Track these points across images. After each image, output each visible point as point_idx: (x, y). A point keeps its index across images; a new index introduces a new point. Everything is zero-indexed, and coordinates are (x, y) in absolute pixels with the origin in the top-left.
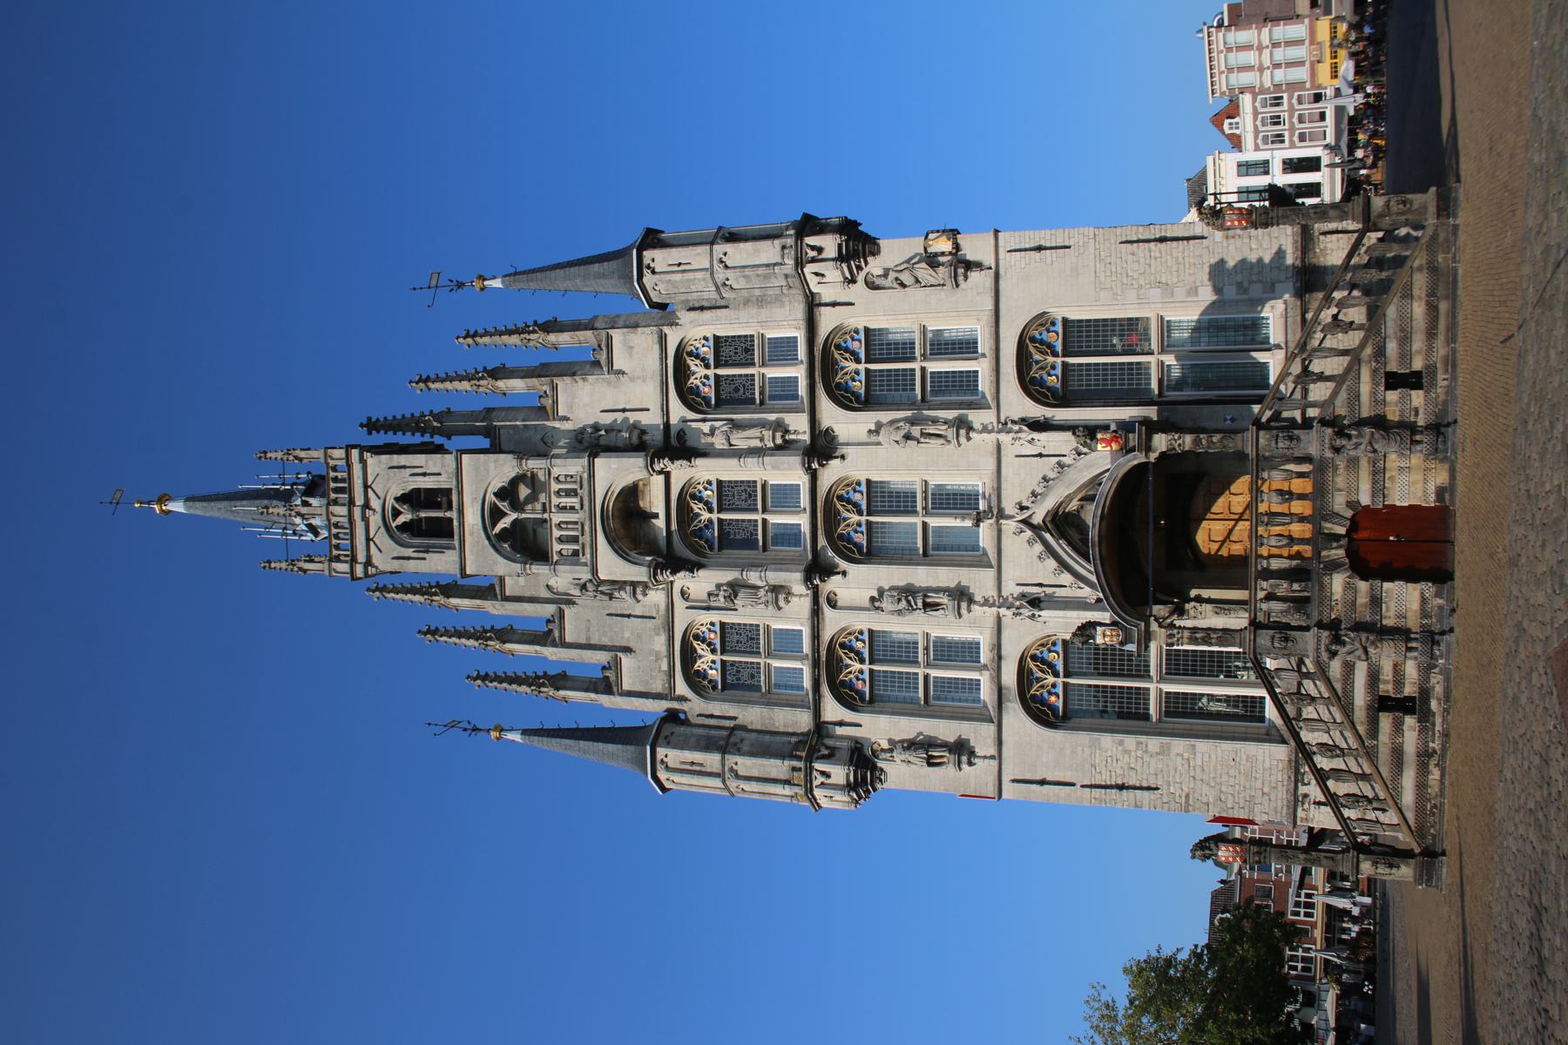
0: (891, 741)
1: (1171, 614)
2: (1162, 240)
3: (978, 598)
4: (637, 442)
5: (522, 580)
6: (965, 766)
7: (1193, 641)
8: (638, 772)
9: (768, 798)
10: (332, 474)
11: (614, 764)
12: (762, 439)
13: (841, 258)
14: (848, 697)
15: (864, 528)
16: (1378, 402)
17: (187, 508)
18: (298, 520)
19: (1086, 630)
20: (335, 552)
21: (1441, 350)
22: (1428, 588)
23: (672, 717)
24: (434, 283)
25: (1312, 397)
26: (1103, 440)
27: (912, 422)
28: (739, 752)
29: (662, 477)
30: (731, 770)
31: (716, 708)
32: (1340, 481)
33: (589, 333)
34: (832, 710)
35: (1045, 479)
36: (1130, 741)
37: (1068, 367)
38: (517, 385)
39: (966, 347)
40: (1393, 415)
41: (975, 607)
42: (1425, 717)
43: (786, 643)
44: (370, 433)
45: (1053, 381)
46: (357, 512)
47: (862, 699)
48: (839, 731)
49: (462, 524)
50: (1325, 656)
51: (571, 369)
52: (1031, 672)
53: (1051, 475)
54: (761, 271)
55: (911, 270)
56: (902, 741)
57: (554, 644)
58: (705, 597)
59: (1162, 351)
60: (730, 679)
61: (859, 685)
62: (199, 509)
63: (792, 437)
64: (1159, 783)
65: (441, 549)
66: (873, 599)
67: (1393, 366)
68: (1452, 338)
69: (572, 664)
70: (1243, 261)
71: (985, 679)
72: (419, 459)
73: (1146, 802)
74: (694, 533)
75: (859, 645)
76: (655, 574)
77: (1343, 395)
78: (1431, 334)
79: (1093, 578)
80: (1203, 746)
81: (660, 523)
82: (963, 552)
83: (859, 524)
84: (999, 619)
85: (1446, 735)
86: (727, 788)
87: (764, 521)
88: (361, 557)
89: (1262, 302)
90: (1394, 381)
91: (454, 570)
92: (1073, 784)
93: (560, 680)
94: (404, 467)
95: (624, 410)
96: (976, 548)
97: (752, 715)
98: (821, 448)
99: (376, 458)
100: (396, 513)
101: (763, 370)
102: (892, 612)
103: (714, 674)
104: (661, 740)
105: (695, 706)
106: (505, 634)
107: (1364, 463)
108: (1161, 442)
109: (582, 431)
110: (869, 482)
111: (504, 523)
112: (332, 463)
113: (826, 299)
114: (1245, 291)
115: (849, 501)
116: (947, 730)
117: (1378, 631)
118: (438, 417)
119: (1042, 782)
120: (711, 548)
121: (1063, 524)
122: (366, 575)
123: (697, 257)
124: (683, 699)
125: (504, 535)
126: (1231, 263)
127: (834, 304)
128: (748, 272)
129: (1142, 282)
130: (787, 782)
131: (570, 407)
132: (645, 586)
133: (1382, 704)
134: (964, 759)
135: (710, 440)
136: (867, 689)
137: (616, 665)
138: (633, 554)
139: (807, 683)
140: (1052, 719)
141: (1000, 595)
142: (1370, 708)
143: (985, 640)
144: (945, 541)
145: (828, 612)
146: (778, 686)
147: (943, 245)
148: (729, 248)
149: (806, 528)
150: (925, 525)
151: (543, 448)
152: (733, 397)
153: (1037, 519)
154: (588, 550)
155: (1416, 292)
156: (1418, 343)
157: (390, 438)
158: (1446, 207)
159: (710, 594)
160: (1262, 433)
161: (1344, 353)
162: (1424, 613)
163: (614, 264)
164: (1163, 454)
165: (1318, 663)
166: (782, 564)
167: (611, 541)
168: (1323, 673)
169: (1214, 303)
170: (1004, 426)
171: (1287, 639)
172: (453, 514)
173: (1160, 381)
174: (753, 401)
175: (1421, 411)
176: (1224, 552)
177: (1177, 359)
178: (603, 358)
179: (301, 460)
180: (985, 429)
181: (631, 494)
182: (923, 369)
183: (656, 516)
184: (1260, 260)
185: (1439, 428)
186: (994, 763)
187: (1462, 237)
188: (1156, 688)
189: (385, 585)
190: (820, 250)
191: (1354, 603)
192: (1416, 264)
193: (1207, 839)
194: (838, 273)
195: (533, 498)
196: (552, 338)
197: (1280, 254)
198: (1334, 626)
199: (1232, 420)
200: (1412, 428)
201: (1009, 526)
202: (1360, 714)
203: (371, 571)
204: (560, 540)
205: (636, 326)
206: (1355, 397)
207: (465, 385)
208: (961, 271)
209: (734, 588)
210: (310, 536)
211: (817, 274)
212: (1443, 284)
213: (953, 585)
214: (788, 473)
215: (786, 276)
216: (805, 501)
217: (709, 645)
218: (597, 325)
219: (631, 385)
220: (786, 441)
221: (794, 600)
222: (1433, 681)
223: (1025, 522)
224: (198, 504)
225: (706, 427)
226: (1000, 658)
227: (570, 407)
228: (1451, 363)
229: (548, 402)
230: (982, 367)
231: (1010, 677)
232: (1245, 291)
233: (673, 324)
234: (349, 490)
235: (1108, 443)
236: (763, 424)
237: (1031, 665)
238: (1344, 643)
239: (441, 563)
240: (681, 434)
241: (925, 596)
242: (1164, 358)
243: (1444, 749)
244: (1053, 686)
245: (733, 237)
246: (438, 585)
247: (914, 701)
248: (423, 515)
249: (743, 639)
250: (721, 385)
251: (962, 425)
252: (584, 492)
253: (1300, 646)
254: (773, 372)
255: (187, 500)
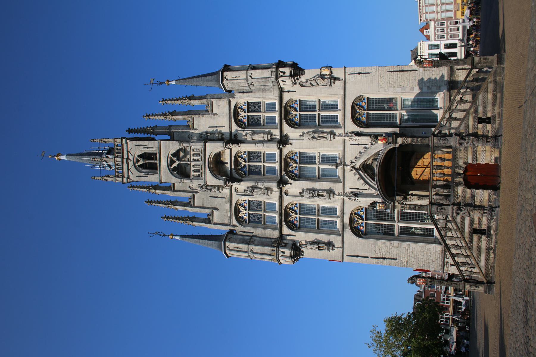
0: (306, 241)
1: (403, 199)
2: (402, 71)
3: (336, 193)
4: (220, 138)
5: (180, 184)
6: (331, 250)
7: (410, 209)
8: (219, 251)
9: (263, 260)
10: (116, 147)
11: (211, 247)
12: (263, 138)
13: (291, 76)
14: (292, 226)
15: (298, 169)
16: (475, 128)
17: (67, 158)
18: (104, 163)
19: (373, 204)
20: (117, 174)
21: (497, 110)
22: (491, 192)
23: (231, 232)
24: (152, 82)
25: (452, 126)
26: (380, 139)
27: (315, 132)
28: (254, 244)
29: (229, 150)
30: (251, 250)
31: (246, 229)
32: (462, 155)
33: (205, 100)
34: (286, 230)
35: (360, 153)
36: (388, 243)
37: (369, 114)
38: (180, 118)
39: (334, 107)
40: (480, 132)
41: (335, 196)
42: (489, 236)
43: (270, 207)
44: (129, 133)
45: (363, 119)
46: (125, 160)
47: (296, 227)
48: (288, 238)
49: (160, 165)
50: (455, 215)
51: (198, 112)
52: (354, 219)
53: (362, 151)
54: (264, 80)
55: (315, 80)
56: (310, 241)
57: (191, 207)
58: (243, 191)
59: (401, 109)
60: (251, 219)
61: (295, 222)
62: (71, 159)
63: (274, 137)
64: (397, 257)
65: (153, 173)
66: (300, 193)
67: (481, 116)
68: (501, 106)
69: (197, 213)
70: (430, 79)
71: (338, 221)
72: (146, 143)
73: (393, 263)
74: (240, 169)
75: (295, 208)
76: (226, 183)
77: (463, 125)
78: (494, 105)
79: (376, 187)
80: (413, 245)
81: (228, 166)
82: (332, 177)
83: (296, 167)
84: (343, 200)
85: (496, 242)
86: (249, 256)
87: (264, 165)
88: (126, 176)
89: (436, 93)
90: (481, 121)
91: (158, 181)
92: (368, 257)
93: (193, 219)
94: (141, 145)
95: (216, 127)
96: (336, 176)
97: (258, 232)
98: (284, 141)
99: (131, 142)
100: (138, 161)
101: (264, 114)
102: (307, 197)
103: (246, 217)
104: (227, 240)
105: (239, 228)
106: (175, 203)
107: (470, 149)
108: (400, 140)
109: (202, 134)
110: (300, 153)
111: (175, 165)
112: (116, 143)
113: (286, 90)
114: (430, 89)
115: (293, 159)
116: (325, 238)
117: (473, 206)
118: (152, 128)
119: (357, 256)
120: (245, 174)
121: (366, 168)
122: (128, 182)
123: (242, 75)
124: (235, 226)
125: (175, 169)
126: (425, 79)
127: (289, 92)
128: (259, 80)
129: (395, 85)
130: (270, 255)
131: (198, 125)
132: (223, 187)
133: (474, 231)
134: (331, 248)
135: (245, 137)
136: (298, 224)
137: (212, 214)
138: (218, 176)
139: (277, 221)
140: (361, 235)
141: (344, 192)
142: (470, 233)
143: (338, 207)
144: (325, 173)
145: (285, 197)
146: (267, 222)
147: (326, 72)
148: (253, 72)
149: (278, 168)
150: (319, 168)
151: (188, 139)
152: (253, 123)
153: (357, 166)
154: (203, 175)
155: (489, 90)
156: (489, 108)
157: (136, 135)
158: (500, 61)
159: (245, 190)
160: (435, 138)
161: (464, 111)
162: (489, 201)
163: (214, 77)
164: (401, 144)
165: (453, 217)
166: (269, 180)
167: (211, 172)
168: (454, 220)
169: (419, 93)
170: (346, 134)
171: (442, 209)
172: (158, 162)
173: (400, 120)
174: (260, 124)
175: (490, 131)
176: (421, 179)
177: (406, 112)
178: (209, 109)
179: (106, 142)
180: (340, 135)
181: (218, 156)
182: (319, 114)
183: (227, 163)
184: (435, 78)
185: (496, 137)
186: (341, 249)
187: (506, 71)
188: (397, 225)
189: (134, 186)
190: (284, 73)
191: (465, 197)
192: (489, 80)
193: (413, 277)
194: (290, 81)
195: (185, 156)
196: (192, 102)
197: (442, 76)
198: (458, 204)
199: (425, 133)
200: (487, 137)
201: (348, 168)
202: (467, 235)
203: (129, 180)
204: (194, 171)
205: (221, 98)
206: (467, 126)
207: (162, 118)
208: (332, 81)
209: (253, 188)
210: (109, 168)
211: (283, 81)
212: (499, 87)
213: (328, 188)
214: (272, 149)
215: (273, 82)
216: (278, 159)
217: (244, 207)
218: (208, 97)
219: (219, 118)
220: (271, 138)
221: (273, 193)
222: (492, 224)
223: (353, 167)
224: (70, 157)
225: (244, 133)
226: (343, 213)
227: (198, 125)
228: (501, 114)
229: (190, 124)
230: (339, 114)
231: (347, 220)
232: (430, 89)
233: (233, 97)
234: (122, 153)
235: (382, 140)
236: (264, 132)
237: (354, 216)
238: (462, 211)
239: (153, 178)
240: (236, 135)
241: (318, 192)
242: (402, 111)
243: (495, 247)
244: (361, 223)
245: (254, 68)
246: (152, 186)
247: (314, 228)
248: (147, 162)
249: (256, 206)
250: (250, 119)
251: (332, 134)
252: (202, 155)
253: (447, 211)
254: (268, 115)
255: (67, 155)
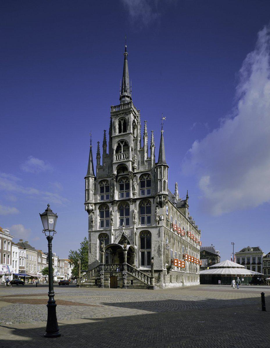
42: (94, 285)
47: (100, 210)
67: (134, 281)
90: (132, 281)
120: (120, 183)
145: (111, 204)
162: (105, 285)
183: (124, 173)
